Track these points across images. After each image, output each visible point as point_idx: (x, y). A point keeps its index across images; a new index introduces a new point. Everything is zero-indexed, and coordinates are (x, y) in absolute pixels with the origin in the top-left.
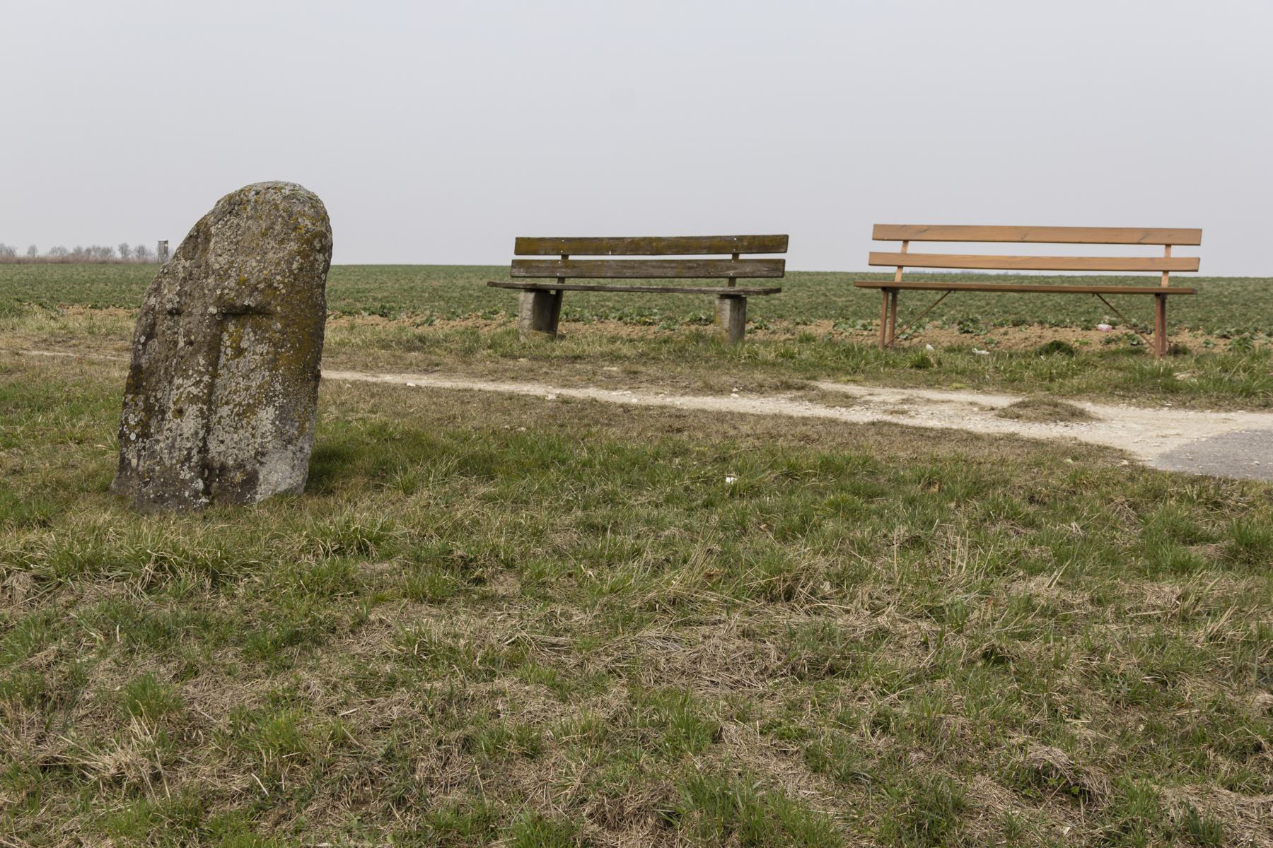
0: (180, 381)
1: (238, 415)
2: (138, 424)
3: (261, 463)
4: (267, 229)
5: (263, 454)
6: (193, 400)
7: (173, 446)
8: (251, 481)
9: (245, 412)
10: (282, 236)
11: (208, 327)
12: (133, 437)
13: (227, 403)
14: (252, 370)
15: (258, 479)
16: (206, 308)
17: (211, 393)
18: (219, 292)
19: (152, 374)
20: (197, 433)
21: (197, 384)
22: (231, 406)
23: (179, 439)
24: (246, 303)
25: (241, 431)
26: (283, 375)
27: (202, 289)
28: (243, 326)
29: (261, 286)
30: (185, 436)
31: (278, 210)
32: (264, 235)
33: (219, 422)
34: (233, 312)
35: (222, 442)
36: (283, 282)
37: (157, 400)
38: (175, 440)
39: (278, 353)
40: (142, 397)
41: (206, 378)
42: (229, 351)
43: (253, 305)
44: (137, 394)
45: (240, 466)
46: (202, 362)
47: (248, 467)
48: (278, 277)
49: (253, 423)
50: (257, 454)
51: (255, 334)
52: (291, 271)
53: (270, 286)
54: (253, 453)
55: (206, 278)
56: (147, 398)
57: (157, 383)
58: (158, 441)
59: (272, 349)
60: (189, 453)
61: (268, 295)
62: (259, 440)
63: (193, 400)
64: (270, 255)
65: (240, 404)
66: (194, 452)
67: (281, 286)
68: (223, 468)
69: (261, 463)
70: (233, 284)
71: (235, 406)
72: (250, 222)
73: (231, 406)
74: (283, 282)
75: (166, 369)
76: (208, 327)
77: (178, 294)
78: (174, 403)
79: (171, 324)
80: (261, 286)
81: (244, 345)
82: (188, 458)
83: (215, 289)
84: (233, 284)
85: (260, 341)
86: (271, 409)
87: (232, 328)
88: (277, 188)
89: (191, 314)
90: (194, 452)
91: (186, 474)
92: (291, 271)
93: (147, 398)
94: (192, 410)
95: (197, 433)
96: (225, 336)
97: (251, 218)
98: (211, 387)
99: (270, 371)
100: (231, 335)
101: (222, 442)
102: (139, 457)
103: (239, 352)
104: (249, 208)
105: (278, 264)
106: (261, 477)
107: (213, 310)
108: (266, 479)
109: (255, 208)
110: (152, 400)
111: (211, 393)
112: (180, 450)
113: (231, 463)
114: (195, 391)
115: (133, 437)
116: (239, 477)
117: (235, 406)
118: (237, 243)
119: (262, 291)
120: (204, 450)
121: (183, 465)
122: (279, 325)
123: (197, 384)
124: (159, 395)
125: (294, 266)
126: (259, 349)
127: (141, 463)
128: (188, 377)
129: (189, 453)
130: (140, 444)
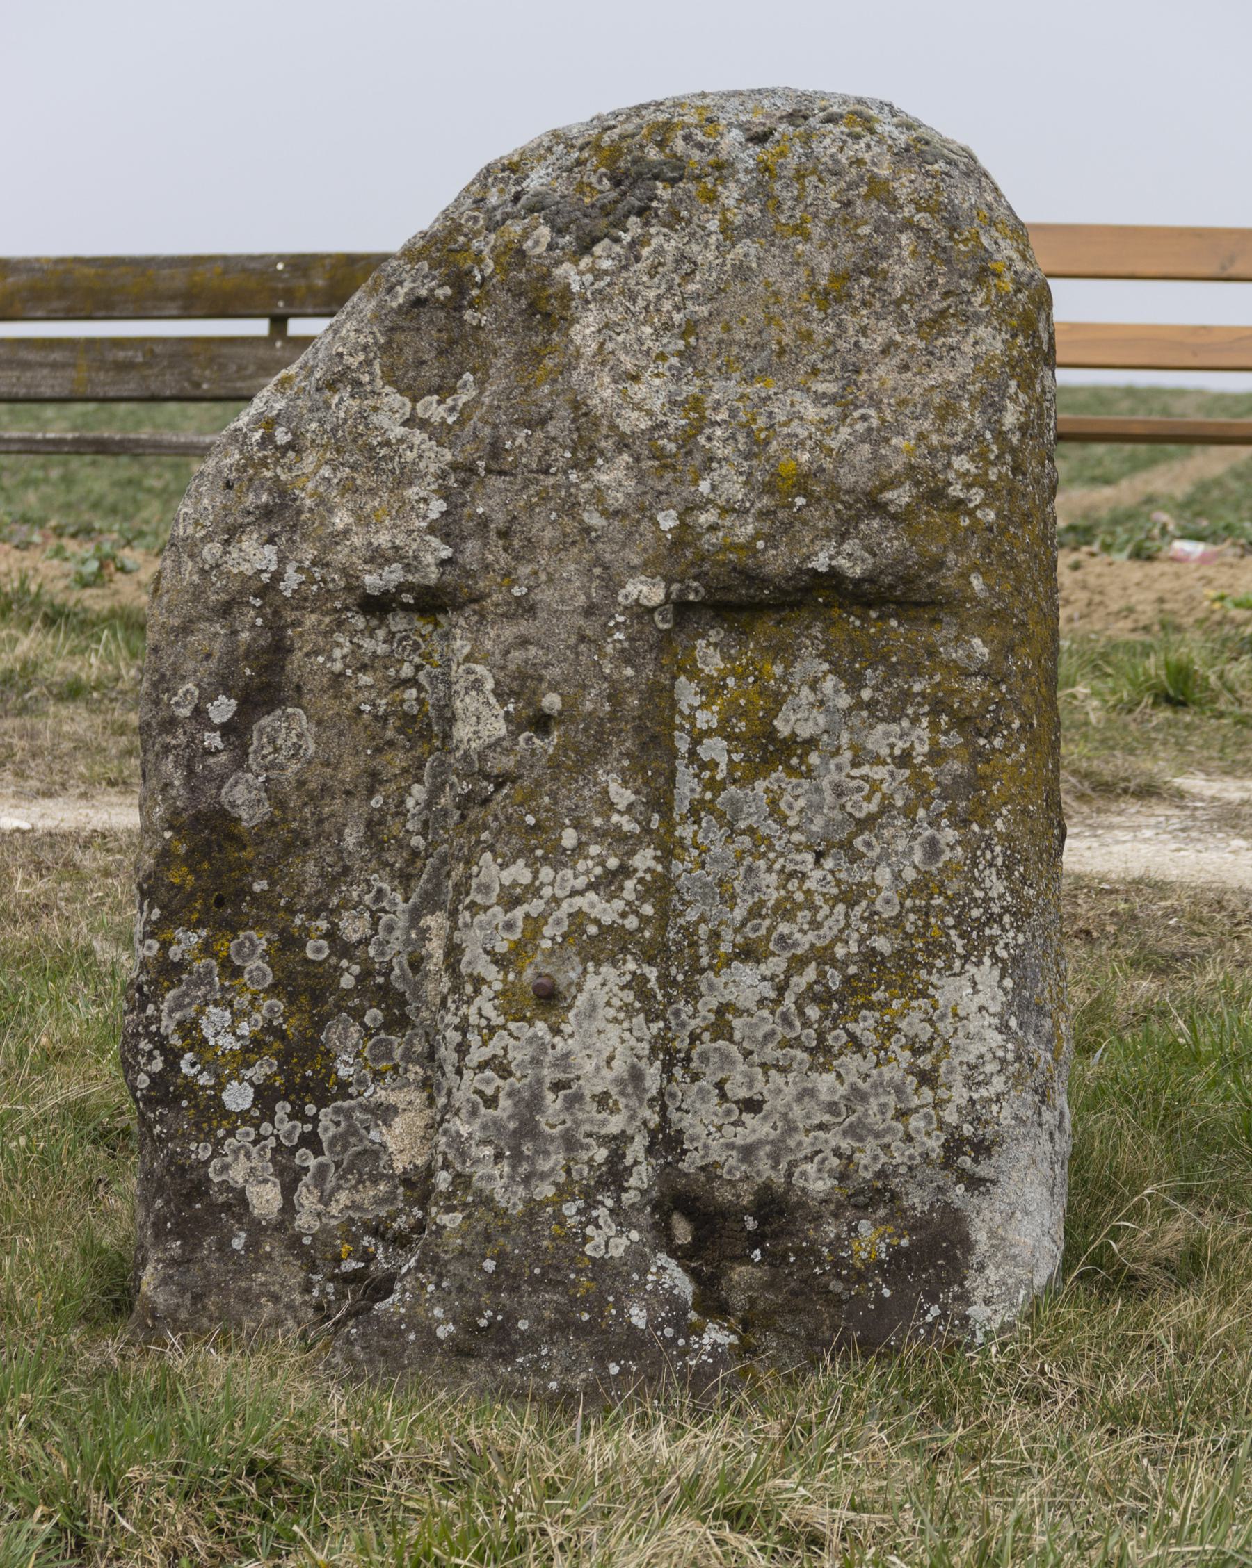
0: (520, 873)
1: (823, 998)
2: (255, 1046)
3: (975, 1183)
4: (843, 277)
5: (982, 1148)
6: (601, 945)
7: (527, 1129)
8: (938, 1253)
10: (935, 302)
11: (626, 657)
12: (238, 1097)
13: (749, 953)
15: (968, 1245)
16: (612, 585)
17: (664, 916)
18: (668, 521)
19: (298, 844)
20: (636, 1076)
21: (608, 883)
22: (776, 965)
23: (553, 1103)
24: (821, 563)
25: (852, 1063)
26: (1008, 838)
27: (571, 507)
28: (784, 652)
29: (900, 496)
30: (591, 1088)
31: (891, 202)
33: (721, 1029)
34: (736, 600)
35: (752, 1105)
36: (980, 481)
37: (342, 948)
38: (534, 1103)
39: (978, 754)
41: (644, 859)
42: (714, 749)
44: (233, 927)
46: (622, 796)
47: (917, 1200)
48: (961, 463)
49: (913, 1024)
50: (954, 1146)
51: (854, 682)
52: (1000, 436)
53: (935, 495)
54: (934, 1144)
55: (584, 465)
56: (290, 942)
57: (333, 882)
58: (384, 1113)
59: (952, 740)
60: (616, 1156)
61: (929, 529)
62: (959, 1094)
63: (601, 945)
64: (884, 374)
65: (823, 956)
66: (636, 1149)
67: (977, 496)
68: (775, 1208)
69: (975, 1183)
70: (735, 490)
71: (798, 964)
72: (746, 248)
73: (776, 965)
74: (980, 481)
75: (373, 825)
76: (626, 657)
77: (444, 529)
78: (501, 961)
79: (375, 645)
80: (900, 496)
82: (614, 1175)
83: (645, 512)
84: (735, 490)
86: (987, 973)
87: (711, 662)
88: (860, 119)
90: (636, 1149)
91: (609, 1241)
92: (1000, 436)
93: (290, 942)
94: (602, 985)
95: (636, 1076)
96: (688, 694)
97: (749, 230)
98: (660, 888)
99: (962, 823)
100: (712, 689)
101: (752, 1105)
102: (290, 1180)
105: (947, 412)
106: (980, 1236)
107: (646, 590)
108: (999, 1242)
110: (317, 950)
111: (664, 916)
113: (818, 1184)
114: (604, 910)
115: (238, 1097)
116: (871, 1239)
118: (690, 328)
119: (901, 518)
120: (666, 1141)
121: (592, 1204)
122: (980, 648)
123: (608, 883)
124: (353, 928)
125: (1010, 418)
127: (306, 1198)
128: (559, 858)
129: (616, 1156)
130: (283, 1124)
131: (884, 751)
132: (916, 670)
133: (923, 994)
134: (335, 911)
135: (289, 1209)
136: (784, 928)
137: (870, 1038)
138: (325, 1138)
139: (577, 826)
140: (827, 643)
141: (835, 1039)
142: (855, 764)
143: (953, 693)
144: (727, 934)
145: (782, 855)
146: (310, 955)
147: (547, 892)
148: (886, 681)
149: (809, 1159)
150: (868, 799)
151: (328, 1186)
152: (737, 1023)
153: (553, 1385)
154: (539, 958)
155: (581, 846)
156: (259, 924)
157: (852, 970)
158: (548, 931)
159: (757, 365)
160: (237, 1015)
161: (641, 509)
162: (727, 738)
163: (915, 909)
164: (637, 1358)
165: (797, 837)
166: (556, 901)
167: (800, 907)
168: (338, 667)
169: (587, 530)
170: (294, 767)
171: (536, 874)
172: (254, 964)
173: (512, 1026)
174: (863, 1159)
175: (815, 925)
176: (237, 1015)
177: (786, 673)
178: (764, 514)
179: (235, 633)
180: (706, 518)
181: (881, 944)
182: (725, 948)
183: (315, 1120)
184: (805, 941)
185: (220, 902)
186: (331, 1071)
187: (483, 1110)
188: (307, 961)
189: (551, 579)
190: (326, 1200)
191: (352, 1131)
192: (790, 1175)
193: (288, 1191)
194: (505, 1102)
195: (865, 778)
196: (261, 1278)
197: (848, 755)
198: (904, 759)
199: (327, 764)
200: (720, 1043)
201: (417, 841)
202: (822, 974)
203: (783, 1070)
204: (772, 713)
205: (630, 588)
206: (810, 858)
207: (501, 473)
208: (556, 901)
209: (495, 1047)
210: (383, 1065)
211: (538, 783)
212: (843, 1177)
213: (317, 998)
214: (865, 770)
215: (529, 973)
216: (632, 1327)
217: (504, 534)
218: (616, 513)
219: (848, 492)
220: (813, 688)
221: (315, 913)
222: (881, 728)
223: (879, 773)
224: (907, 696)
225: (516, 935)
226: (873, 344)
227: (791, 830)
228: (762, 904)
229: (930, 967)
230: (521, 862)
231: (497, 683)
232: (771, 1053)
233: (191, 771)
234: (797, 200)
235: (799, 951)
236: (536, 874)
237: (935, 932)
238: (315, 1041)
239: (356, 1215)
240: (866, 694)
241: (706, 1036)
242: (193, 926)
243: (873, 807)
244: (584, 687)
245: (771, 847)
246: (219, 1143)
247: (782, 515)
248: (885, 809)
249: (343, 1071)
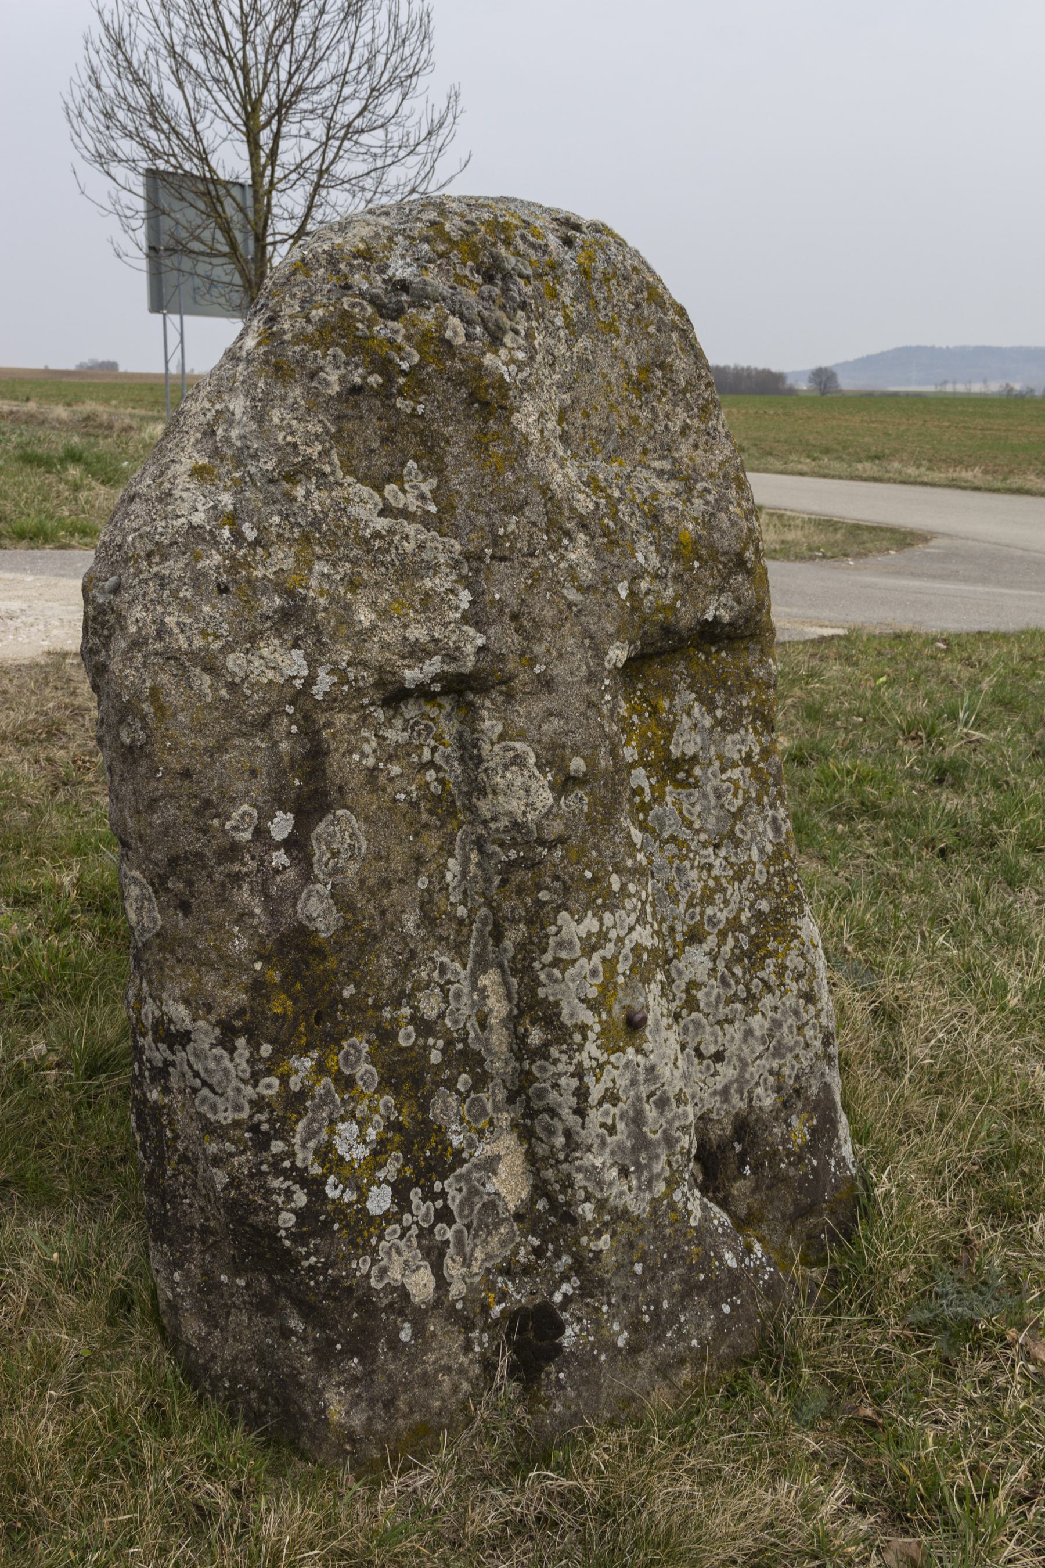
0: (591, 924)
2: (380, 1149)
7: (641, 1143)
9: (757, 943)
12: (380, 1201)
14: (738, 815)
16: (600, 654)
22: (711, 942)
23: (650, 1111)
28: (668, 689)
32: (641, 387)
35: (719, 1057)
37: (425, 1027)
38: (637, 1120)
40: (361, 1043)
43: (726, 617)
44: (334, 1040)
45: (791, 1097)
49: (793, 961)
56: (386, 1035)
57: (404, 968)
58: (490, 1164)
65: (734, 924)
71: (722, 935)
72: (583, 343)
75: (425, 904)
77: (475, 618)
78: (593, 1005)
79: (395, 735)
81: (685, 743)
83: (610, 585)
85: (729, 725)
89: (547, 683)
101: (719, 1057)
102: (435, 1255)
103: (674, 770)
104: (567, 293)
109: (583, 294)
112: (670, 1142)
117: (722, 935)
124: (430, 1006)
126: (734, 746)
127: (453, 1268)
128: (612, 902)
130: (421, 1208)
131: (736, 757)
132: (742, 690)
133: (795, 936)
134: (411, 996)
135: (442, 1283)
136: (709, 911)
137: (773, 980)
138: (454, 1207)
139: (617, 871)
140: (693, 677)
141: (756, 985)
142: (723, 770)
143: (763, 703)
144: (679, 927)
145: (696, 853)
146: (403, 1043)
147: (613, 934)
148: (728, 701)
149: (757, 1084)
150: (735, 795)
151: (468, 1249)
152: (700, 995)
153: (694, 1342)
154: (621, 994)
155: (624, 887)
156: (357, 1028)
157: (753, 931)
158: (620, 968)
159: (611, 446)
160: (363, 1123)
161: (605, 583)
162: (645, 767)
163: (777, 874)
164: (736, 1293)
165: (703, 837)
166: (620, 940)
167: (714, 891)
168: (371, 762)
169: (570, 605)
170: (353, 868)
171: (601, 920)
172: (363, 1068)
173: (613, 1058)
174: (786, 1071)
175: (726, 902)
176: (363, 1123)
177: (672, 706)
178: (677, 577)
179: (275, 744)
180: (644, 585)
181: (764, 906)
182: (679, 938)
183: (443, 1194)
184: (722, 916)
185: (319, 1019)
186: (446, 1144)
187: (609, 1139)
188: (401, 1050)
189: (560, 655)
190: (467, 1263)
191: (473, 1192)
192: (751, 1100)
193: (437, 1270)
194: (621, 1126)
195: (730, 780)
196: (431, 1357)
197: (717, 763)
198: (748, 760)
199: (380, 858)
200: (694, 1015)
201: (462, 911)
202: (736, 939)
203: (731, 1022)
204: (668, 740)
205: (611, 653)
206: (710, 850)
207: (503, 559)
208: (620, 940)
209: (606, 1082)
210: (483, 1123)
211: (584, 840)
212: (779, 1089)
213: (417, 1082)
214: (729, 773)
215: (616, 1009)
216: (730, 1269)
217: (515, 617)
218: (589, 587)
219: (724, 554)
220: (689, 715)
221: (397, 1004)
222: (729, 738)
223: (735, 773)
224: (741, 709)
225: (600, 980)
226: (675, 427)
227: (697, 832)
228: (693, 895)
229: (793, 914)
230: (590, 913)
231: (537, 756)
232: (723, 1011)
233: (268, 896)
234: (607, 300)
235: (721, 926)
236: (601, 920)
237: (791, 888)
238: (426, 1122)
239: (488, 1265)
240: (719, 713)
241: (684, 1012)
242: (304, 1052)
243: (739, 802)
244: (596, 747)
245: (689, 850)
246: (375, 1251)
247: (686, 576)
248: (746, 800)
249: (456, 1141)
